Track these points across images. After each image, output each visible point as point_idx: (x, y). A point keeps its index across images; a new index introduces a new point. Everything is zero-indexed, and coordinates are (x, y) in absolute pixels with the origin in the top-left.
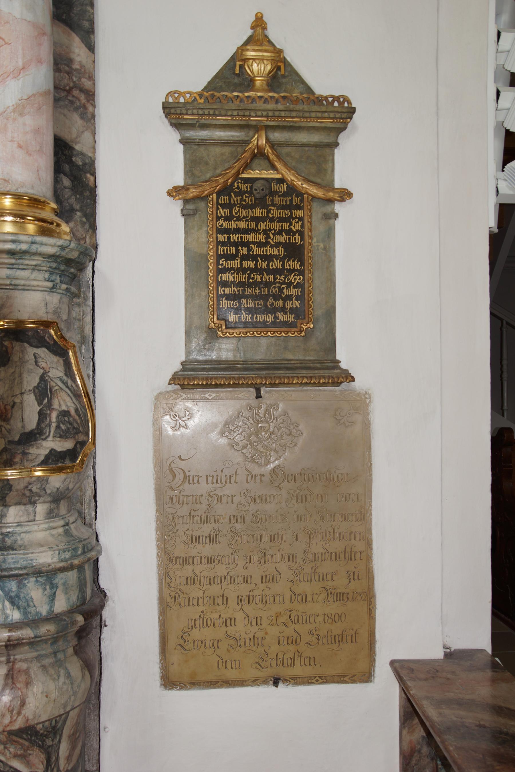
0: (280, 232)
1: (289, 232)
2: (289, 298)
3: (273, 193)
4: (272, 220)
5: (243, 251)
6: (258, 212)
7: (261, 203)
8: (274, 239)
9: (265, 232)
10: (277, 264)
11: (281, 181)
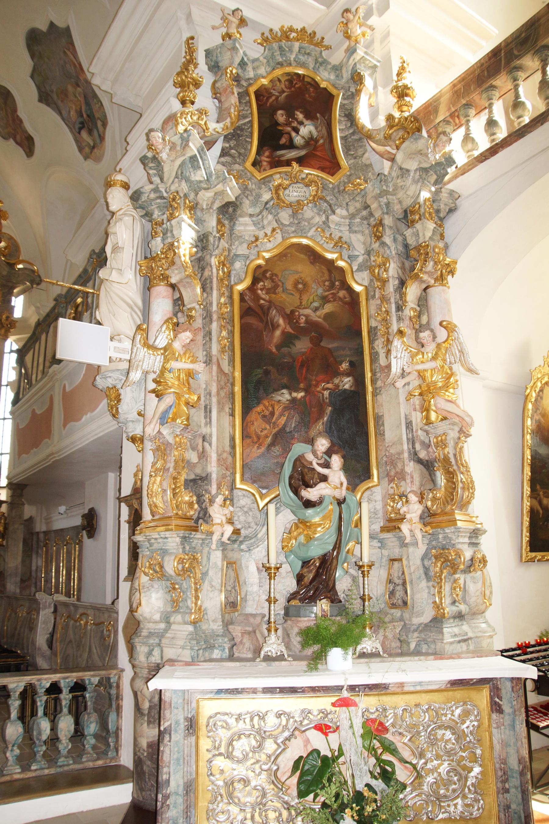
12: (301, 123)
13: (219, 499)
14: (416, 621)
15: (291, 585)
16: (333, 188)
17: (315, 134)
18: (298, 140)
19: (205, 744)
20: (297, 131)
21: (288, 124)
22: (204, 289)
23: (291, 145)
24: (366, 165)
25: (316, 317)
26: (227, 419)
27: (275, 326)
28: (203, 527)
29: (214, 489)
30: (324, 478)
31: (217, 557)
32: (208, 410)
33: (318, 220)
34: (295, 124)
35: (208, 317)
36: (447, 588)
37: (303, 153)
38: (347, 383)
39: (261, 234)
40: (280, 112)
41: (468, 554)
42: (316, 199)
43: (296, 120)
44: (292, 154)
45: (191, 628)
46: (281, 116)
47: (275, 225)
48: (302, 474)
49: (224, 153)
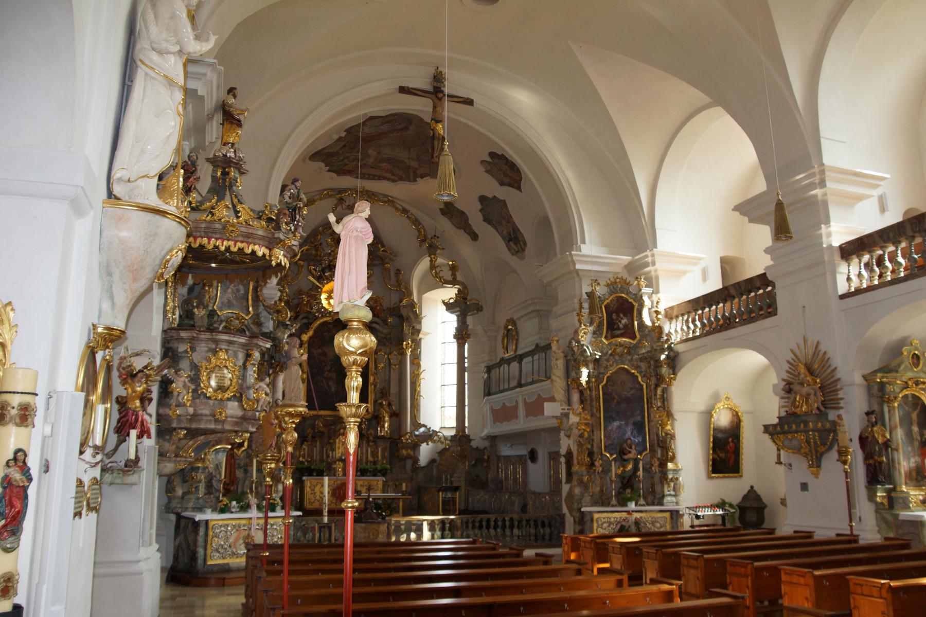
12: (622, 319)
13: (598, 459)
14: (657, 496)
15: (620, 485)
16: (633, 347)
17: (627, 323)
18: (621, 326)
19: (595, 525)
20: (620, 322)
21: (617, 319)
22: (590, 390)
23: (619, 329)
24: (647, 335)
25: (629, 395)
26: (599, 432)
27: (614, 398)
28: (594, 468)
29: (595, 456)
30: (630, 452)
31: (597, 476)
32: (593, 431)
33: (629, 357)
34: (620, 319)
35: (592, 400)
36: (666, 487)
37: (623, 331)
38: (639, 418)
39: (608, 364)
40: (614, 314)
41: (670, 477)
42: (629, 353)
43: (620, 317)
44: (619, 332)
45: (590, 497)
46: (614, 316)
47: (613, 360)
48: (623, 451)
49: (594, 333)
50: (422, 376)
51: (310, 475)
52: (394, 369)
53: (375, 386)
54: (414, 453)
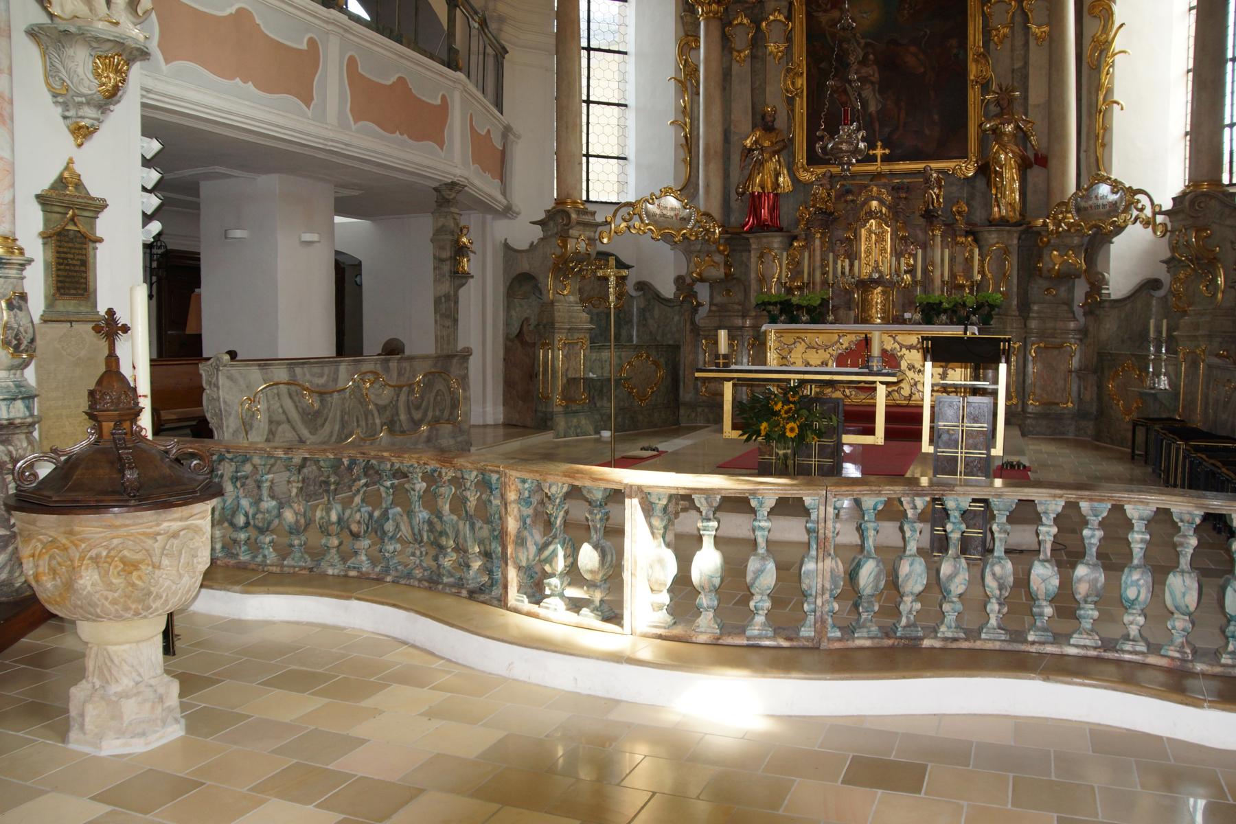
0: (78, 254)
1: (82, 255)
2: (82, 283)
3: (76, 237)
4: (75, 248)
5: (66, 262)
6: (71, 245)
7: (71, 241)
8: (77, 257)
9: (74, 254)
10: (77, 268)
11: (79, 231)
50: (1117, 45)
51: (794, 320)
52: (1037, 38)
53: (985, 88)
54: (1090, 259)
